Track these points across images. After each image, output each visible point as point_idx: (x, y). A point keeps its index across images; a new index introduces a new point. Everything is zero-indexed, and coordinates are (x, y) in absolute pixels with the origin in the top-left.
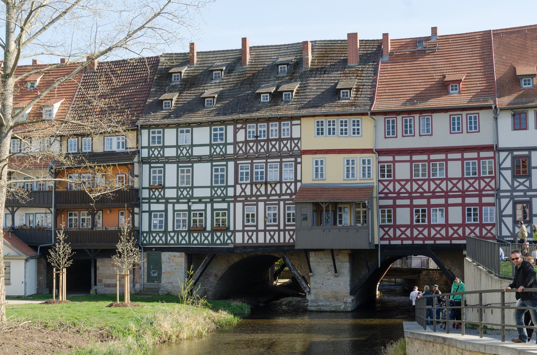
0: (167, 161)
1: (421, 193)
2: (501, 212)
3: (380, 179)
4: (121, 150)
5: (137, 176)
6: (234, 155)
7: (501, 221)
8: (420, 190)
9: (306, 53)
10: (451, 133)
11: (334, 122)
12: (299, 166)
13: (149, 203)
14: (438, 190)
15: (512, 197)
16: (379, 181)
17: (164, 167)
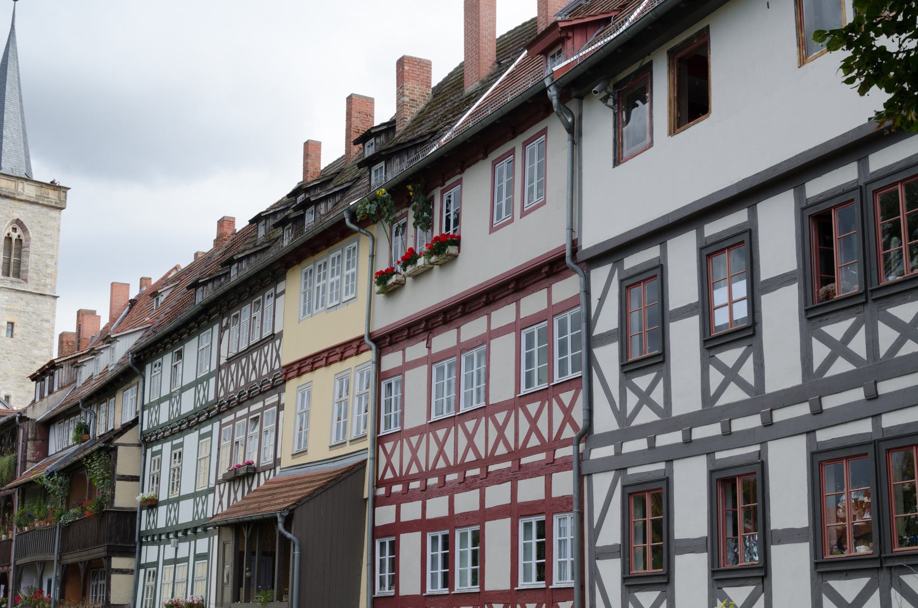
0: (163, 437)
1: (442, 474)
2: (595, 533)
3: (383, 432)
4: (133, 417)
5: (135, 479)
6: (216, 404)
7: (595, 574)
8: (441, 464)
9: (401, 90)
10: (492, 229)
11: (325, 264)
12: (281, 413)
13: (147, 544)
14: (471, 457)
15: (619, 465)
16: (379, 441)
17: (160, 452)
